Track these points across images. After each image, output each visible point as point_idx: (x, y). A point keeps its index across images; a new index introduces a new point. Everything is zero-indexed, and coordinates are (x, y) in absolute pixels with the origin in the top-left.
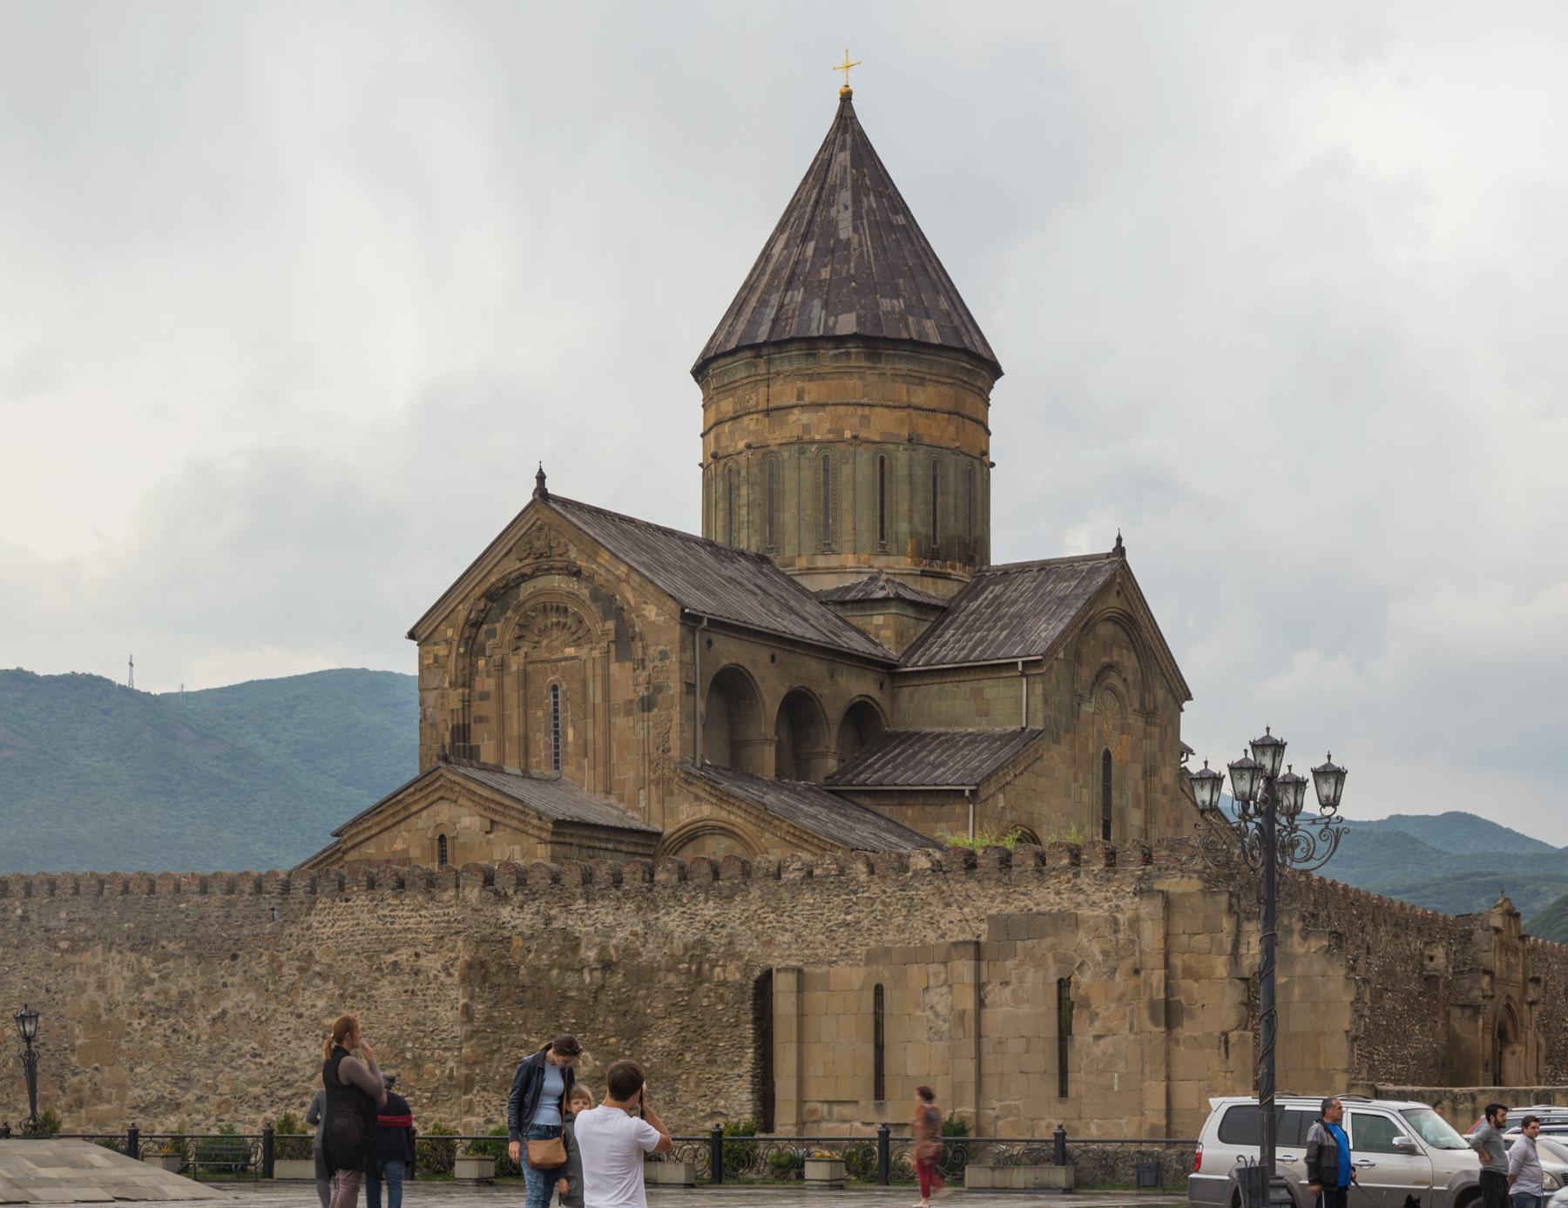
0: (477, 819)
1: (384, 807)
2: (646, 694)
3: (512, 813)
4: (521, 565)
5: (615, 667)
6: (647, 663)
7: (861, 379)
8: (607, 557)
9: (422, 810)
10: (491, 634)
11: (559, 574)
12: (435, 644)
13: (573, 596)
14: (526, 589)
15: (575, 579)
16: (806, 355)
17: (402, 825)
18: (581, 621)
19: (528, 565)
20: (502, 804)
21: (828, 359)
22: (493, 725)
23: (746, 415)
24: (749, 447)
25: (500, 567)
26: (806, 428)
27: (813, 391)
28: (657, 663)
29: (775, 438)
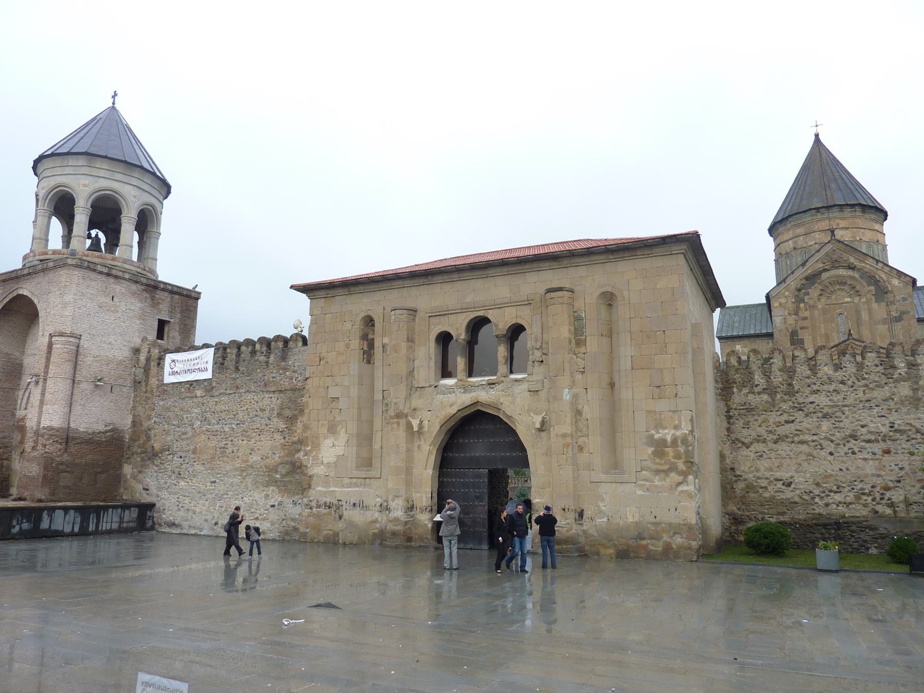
2: (897, 315)
4: (825, 265)
5: (875, 305)
6: (895, 302)
7: (861, 220)
10: (808, 294)
12: (779, 298)
14: (825, 275)
15: (851, 270)
16: (840, 211)
21: (848, 212)
22: (810, 330)
24: (815, 244)
25: (812, 267)
26: (842, 236)
28: (901, 302)
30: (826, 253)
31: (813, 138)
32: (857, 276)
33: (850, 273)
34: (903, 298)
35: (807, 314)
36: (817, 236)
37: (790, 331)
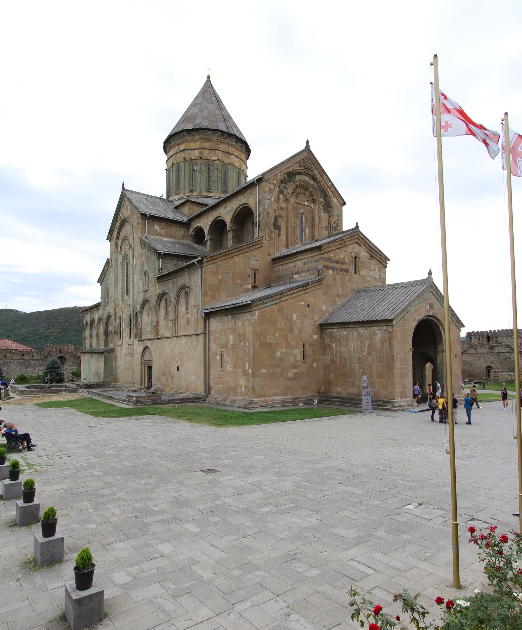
0: (366, 254)
1: (339, 240)
3: (378, 254)
5: (322, 214)
8: (326, 178)
9: (350, 244)
11: (308, 177)
12: (269, 183)
13: (313, 186)
14: (298, 177)
16: (236, 142)
17: (343, 249)
18: (312, 195)
19: (302, 169)
20: (375, 250)
23: (217, 150)
24: (218, 160)
27: (236, 153)
28: (337, 217)
29: (227, 161)
30: (302, 159)
31: (206, 78)
32: (316, 187)
33: (312, 182)
34: (338, 214)
35: (284, 205)
36: (219, 154)
37: (275, 216)
